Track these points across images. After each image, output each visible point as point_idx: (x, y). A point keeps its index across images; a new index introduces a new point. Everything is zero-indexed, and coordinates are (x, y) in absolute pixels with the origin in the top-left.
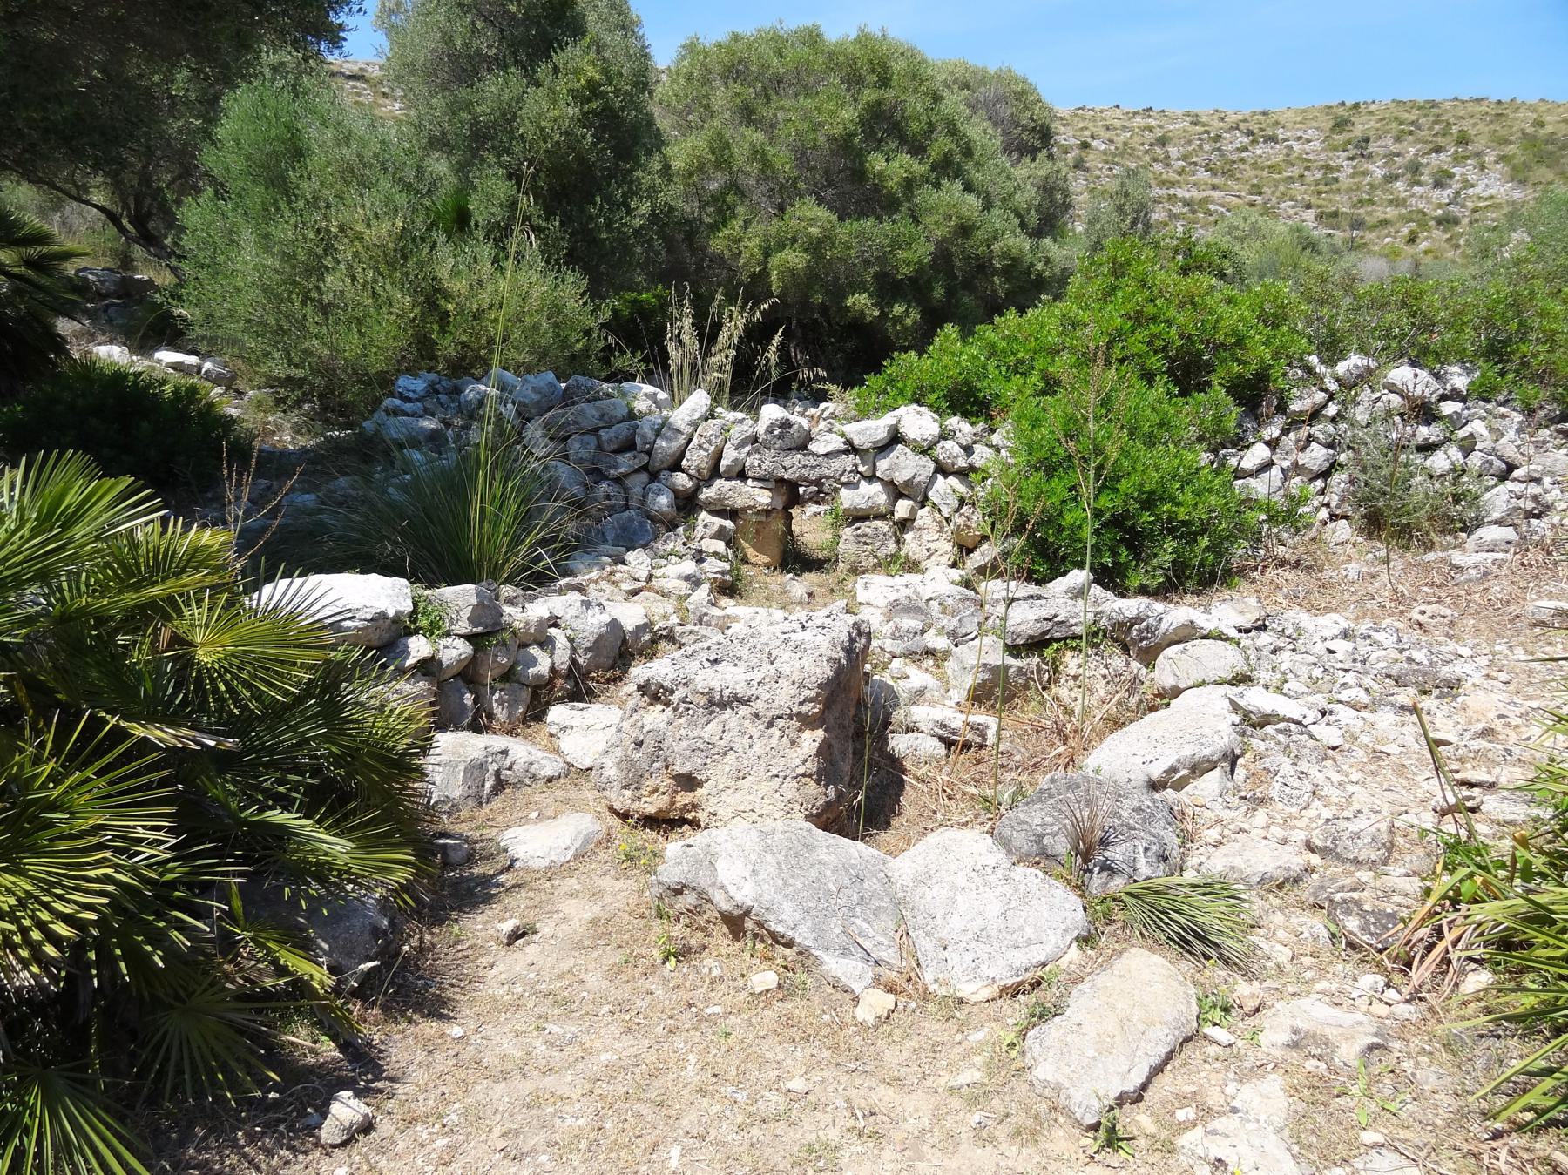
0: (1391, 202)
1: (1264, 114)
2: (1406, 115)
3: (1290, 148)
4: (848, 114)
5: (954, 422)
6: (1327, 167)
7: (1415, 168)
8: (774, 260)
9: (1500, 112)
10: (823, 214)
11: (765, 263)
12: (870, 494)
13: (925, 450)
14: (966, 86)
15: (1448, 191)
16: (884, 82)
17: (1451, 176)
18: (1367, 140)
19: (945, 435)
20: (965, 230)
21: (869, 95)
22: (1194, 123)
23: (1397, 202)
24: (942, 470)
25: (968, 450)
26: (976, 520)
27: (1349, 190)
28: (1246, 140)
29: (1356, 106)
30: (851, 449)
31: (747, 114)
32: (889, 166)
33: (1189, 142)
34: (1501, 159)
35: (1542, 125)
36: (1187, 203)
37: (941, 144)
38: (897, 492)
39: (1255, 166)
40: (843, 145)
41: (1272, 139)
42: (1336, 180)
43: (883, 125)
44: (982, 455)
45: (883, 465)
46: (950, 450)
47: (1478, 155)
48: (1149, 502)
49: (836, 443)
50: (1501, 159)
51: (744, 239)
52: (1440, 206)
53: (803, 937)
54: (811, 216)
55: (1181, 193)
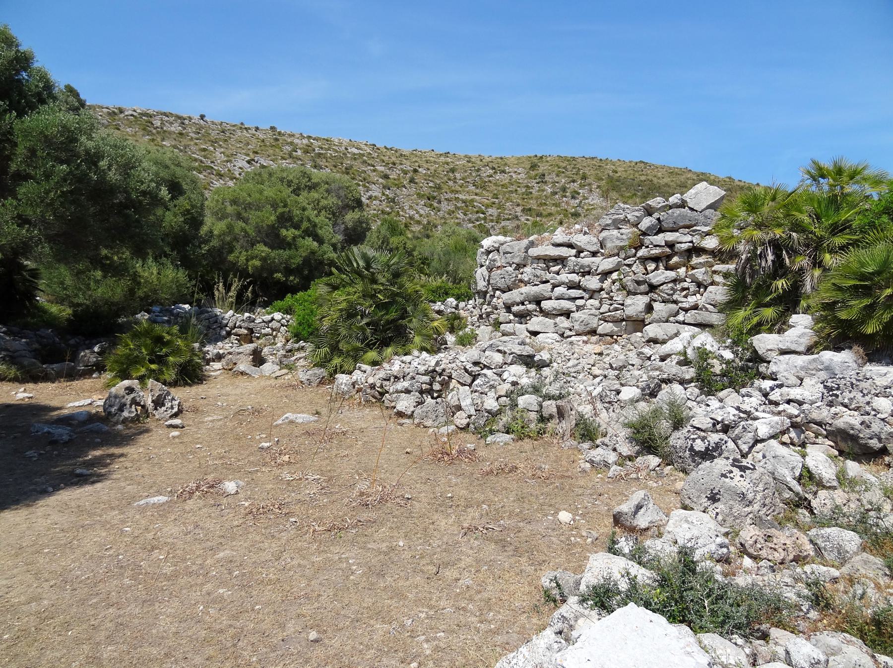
0: (554, 204)
1: (501, 158)
2: (561, 164)
3: (511, 176)
4: (273, 218)
6: (527, 187)
7: (564, 189)
9: (600, 164)
10: (266, 249)
12: (268, 330)
13: (279, 321)
14: (327, 183)
15: (577, 201)
16: (285, 206)
17: (579, 194)
18: (544, 175)
19: (283, 318)
20: (313, 253)
21: (280, 210)
22: (468, 162)
23: (556, 205)
24: (282, 325)
25: (288, 321)
27: (537, 198)
28: (491, 171)
29: (541, 158)
30: (264, 322)
31: (239, 216)
32: (288, 233)
33: (466, 171)
34: (599, 187)
35: (616, 172)
36: (464, 202)
37: (305, 225)
38: (273, 330)
39: (496, 184)
40: (272, 227)
41: (504, 172)
42: (531, 193)
43: (285, 220)
47: (590, 184)
49: (261, 320)
50: (599, 187)
51: (239, 256)
52: (574, 207)
54: (262, 249)
55: (461, 196)
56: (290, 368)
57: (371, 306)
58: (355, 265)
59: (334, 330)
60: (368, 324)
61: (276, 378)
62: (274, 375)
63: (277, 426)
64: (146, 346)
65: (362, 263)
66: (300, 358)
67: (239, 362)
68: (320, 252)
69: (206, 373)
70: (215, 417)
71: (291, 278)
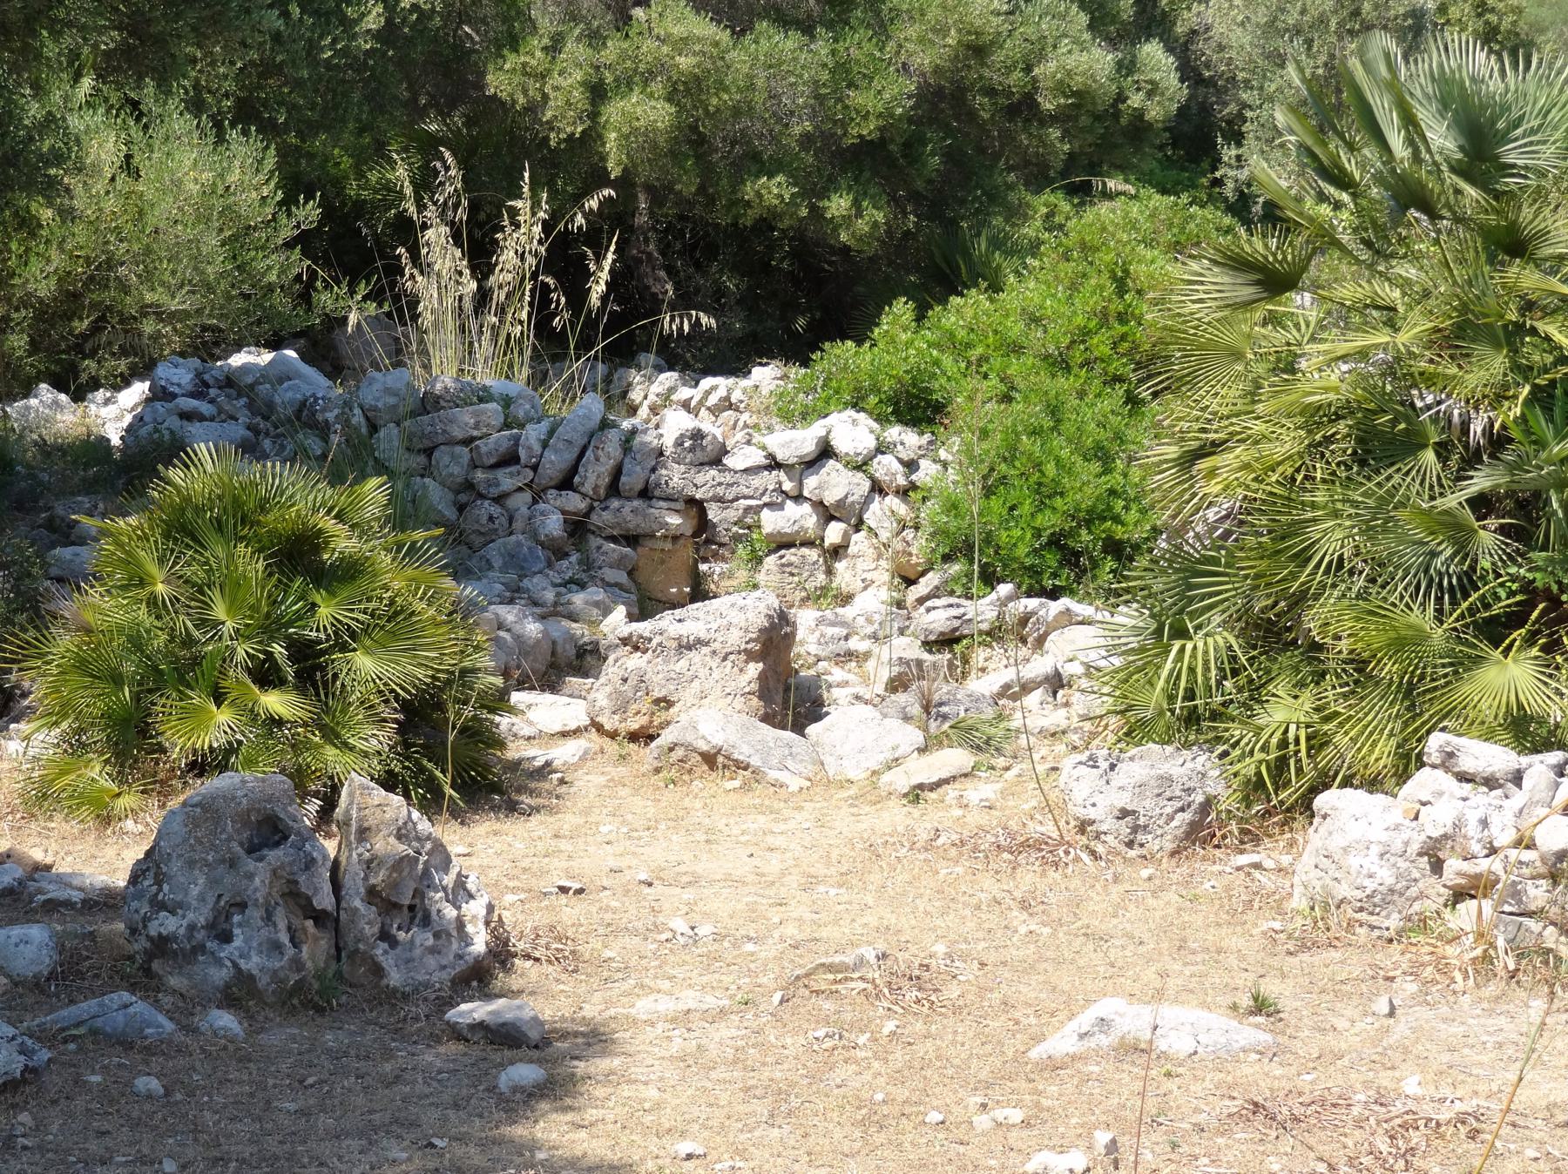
5: (894, 432)
8: (614, 111)
11: (594, 115)
12: (797, 517)
13: (861, 466)
19: (881, 449)
25: (911, 466)
26: (919, 546)
30: (774, 464)
38: (828, 514)
44: (927, 472)
45: (811, 483)
46: (888, 466)
48: (1091, 519)
49: (756, 457)
53: (755, 761)
56: (984, 740)
57: (1500, 397)
58: (1396, 141)
59: (1275, 527)
60: (1482, 504)
61: (916, 794)
62: (901, 780)
63: (1053, 1066)
64: (233, 587)
65: (1442, 139)
66: (1026, 688)
67: (687, 695)
68: (1011, 49)
69: (513, 752)
70: (689, 999)
71: (838, 205)
